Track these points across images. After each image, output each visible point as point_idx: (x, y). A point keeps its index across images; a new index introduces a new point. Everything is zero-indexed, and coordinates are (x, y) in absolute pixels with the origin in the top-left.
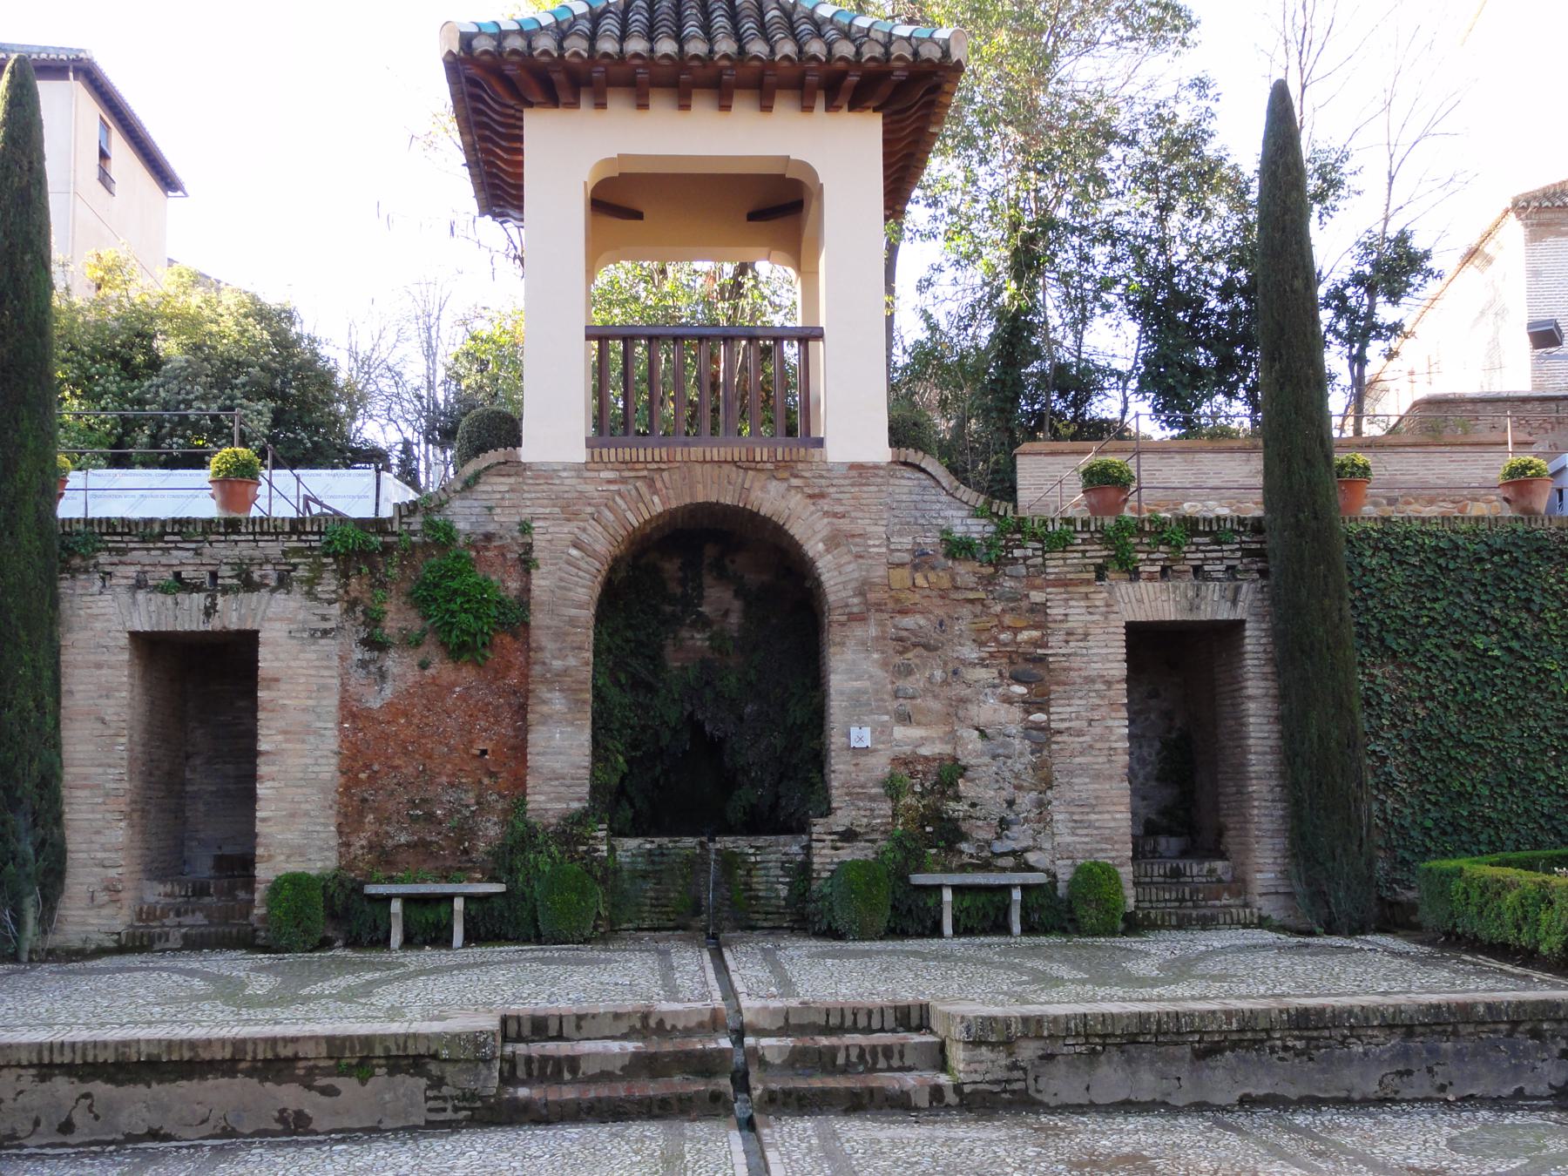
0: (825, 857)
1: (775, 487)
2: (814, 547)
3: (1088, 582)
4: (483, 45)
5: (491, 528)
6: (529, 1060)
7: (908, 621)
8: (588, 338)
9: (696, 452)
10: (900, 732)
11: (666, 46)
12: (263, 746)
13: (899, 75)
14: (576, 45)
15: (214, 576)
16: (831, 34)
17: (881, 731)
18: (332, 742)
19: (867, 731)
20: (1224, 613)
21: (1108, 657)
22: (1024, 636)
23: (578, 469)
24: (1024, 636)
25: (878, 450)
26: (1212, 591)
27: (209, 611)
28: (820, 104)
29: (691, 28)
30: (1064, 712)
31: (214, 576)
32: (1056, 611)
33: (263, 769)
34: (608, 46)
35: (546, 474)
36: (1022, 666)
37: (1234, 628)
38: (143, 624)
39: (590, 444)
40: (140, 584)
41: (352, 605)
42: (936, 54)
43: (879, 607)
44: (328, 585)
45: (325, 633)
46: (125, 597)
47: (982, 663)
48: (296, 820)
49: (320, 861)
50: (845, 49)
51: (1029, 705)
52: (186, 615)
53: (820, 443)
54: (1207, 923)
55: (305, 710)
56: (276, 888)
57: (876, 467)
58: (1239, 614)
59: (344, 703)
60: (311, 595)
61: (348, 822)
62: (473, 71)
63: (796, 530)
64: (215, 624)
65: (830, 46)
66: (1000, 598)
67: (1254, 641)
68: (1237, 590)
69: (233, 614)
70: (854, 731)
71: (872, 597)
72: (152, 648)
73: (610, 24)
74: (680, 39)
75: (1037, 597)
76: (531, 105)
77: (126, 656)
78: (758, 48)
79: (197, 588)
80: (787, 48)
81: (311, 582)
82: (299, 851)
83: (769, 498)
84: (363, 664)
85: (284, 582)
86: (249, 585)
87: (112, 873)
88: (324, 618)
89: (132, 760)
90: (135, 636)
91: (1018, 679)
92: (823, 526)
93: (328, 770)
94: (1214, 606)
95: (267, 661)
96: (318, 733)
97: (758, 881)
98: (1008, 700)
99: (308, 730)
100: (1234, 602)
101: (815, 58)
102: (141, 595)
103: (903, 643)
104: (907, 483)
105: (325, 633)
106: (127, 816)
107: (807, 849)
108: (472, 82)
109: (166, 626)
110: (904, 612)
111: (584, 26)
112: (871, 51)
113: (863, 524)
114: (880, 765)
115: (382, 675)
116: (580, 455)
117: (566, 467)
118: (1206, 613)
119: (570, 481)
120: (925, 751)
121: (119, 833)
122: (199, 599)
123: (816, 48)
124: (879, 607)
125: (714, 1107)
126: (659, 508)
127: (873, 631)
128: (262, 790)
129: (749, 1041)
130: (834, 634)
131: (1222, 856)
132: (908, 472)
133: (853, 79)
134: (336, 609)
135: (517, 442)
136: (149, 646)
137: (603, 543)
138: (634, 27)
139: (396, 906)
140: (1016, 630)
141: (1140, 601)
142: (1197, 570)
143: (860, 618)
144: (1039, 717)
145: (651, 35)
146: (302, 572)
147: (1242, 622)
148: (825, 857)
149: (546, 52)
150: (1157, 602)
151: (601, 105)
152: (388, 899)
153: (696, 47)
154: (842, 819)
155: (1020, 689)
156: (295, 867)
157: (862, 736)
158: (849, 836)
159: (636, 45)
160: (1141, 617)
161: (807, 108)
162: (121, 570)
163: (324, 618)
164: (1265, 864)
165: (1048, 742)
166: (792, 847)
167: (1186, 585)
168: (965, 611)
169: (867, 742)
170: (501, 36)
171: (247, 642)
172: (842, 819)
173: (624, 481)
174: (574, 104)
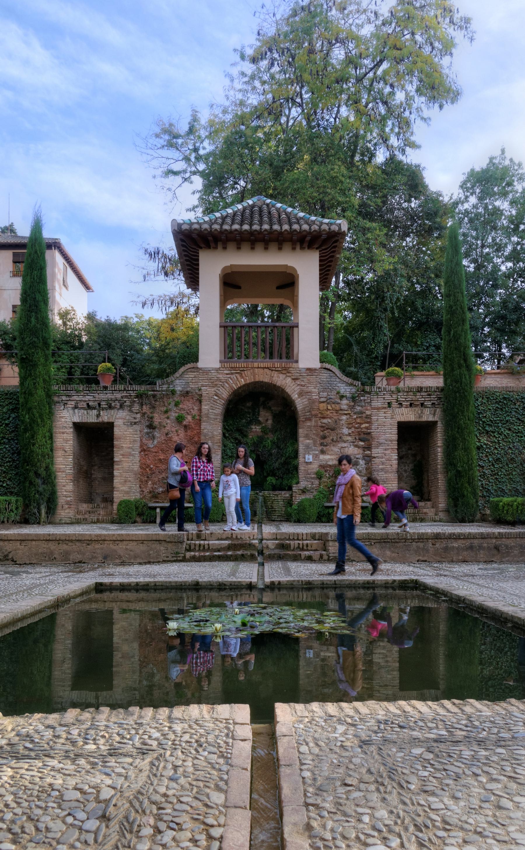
0: (298, 499)
1: (282, 376)
2: (295, 397)
3: (385, 408)
4: (185, 227)
5: (188, 389)
6: (200, 545)
7: (325, 421)
8: (221, 327)
9: (256, 365)
10: (322, 457)
11: (246, 227)
12: (116, 459)
13: (324, 236)
14: (216, 227)
15: (99, 405)
16: (302, 222)
17: (316, 457)
18: (137, 458)
19: (311, 457)
20: (431, 419)
21: (393, 434)
22: (364, 426)
23: (217, 370)
24: (364, 426)
25: (316, 364)
26: (427, 411)
27: (98, 416)
28: (298, 247)
29: (256, 220)
30: (375, 452)
31: (99, 405)
32: (374, 418)
33: (116, 467)
34: (226, 227)
35: (206, 371)
36: (362, 436)
37: (435, 423)
38: (77, 419)
39: (221, 362)
40: (76, 407)
41: (144, 414)
42: (337, 228)
43: (316, 416)
44: (136, 407)
45: (135, 423)
46: (71, 412)
47: (349, 435)
48: (126, 484)
49: (135, 495)
50: (305, 227)
51: (365, 448)
52: (91, 417)
53: (297, 362)
54: (422, 520)
55: (129, 448)
56: (120, 504)
57: (315, 369)
58: (436, 419)
59: (141, 446)
60: (131, 411)
61: (143, 483)
62: (182, 237)
63: (288, 390)
64: (100, 420)
65: (300, 227)
66: (355, 413)
67: (440, 428)
68: (435, 411)
69: (106, 417)
70: (307, 456)
71: (313, 413)
72: (78, 427)
73: (229, 220)
74: (251, 225)
75: (368, 413)
76: (201, 248)
77: (72, 430)
78: (276, 227)
79: (94, 408)
80: (286, 227)
81: (130, 406)
82: (127, 493)
83: (281, 380)
84: (148, 433)
85: (122, 407)
86: (110, 407)
87: (69, 499)
88: (135, 418)
89: (74, 464)
90: (75, 424)
91: (361, 440)
92: (297, 389)
93: (136, 467)
94: (427, 416)
95: (117, 431)
96: (133, 455)
97: (275, 506)
98: (356, 446)
99: (130, 454)
100: (434, 414)
101: (295, 230)
102: (76, 411)
103: (324, 428)
104: (325, 376)
105: (135, 423)
106: (73, 481)
107: (291, 496)
108: (182, 240)
109: (85, 420)
110: (324, 418)
111: (220, 221)
112: (315, 227)
113: (311, 388)
114: (315, 467)
115: (154, 438)
116: (218, 365)
117: (213, 369)
118: (424, 419)
119: (214, 374)
120: (330, 463)
121: (70, 487)
122: (95, 412)
123: (296, 227)
124: (316, 416)
125: (252, 558)
126: (243, 382)
127: (313, 423)
128: (116, 473)
129: (264, 542)
130: (300, 425)
131: (429, 500)
132: (326, 371)
133: (308, 238)
134: (139, 416)
135: (196, 360)
136: (78, 427)
137: (225, 394)
138: (237, 221)
139: (158, 510)
140: (361, 424)
141: (403, 415)
142: (422, 405)
143: (310, 419)
144: (368, 452)
145: (241, 224)
146: (128, 403)
147: (437, 422)
148: (298, 499)
149: (206, 230)
150: (409, 415)
151: (225, 248)
152: (155, 508)
153: (256, 227)
154: (303, 484)
155: (362, 443)
156: (126, 498)
157: (309, 458)
158: (304, 491)
159: (236, 227)
160: (403, 419)
161: (294, 249)
162: (69, 402)
163: (135, 418)
164: (442, 502)
165: (370, 461)
166: (286, 494)
167: (418, 410)
168: (344, 417)
169: (311, 460)
170: (191, 224)
171: (111, 425)
172: (303, 484)
173: (232, 374)
174: (216, 248)
